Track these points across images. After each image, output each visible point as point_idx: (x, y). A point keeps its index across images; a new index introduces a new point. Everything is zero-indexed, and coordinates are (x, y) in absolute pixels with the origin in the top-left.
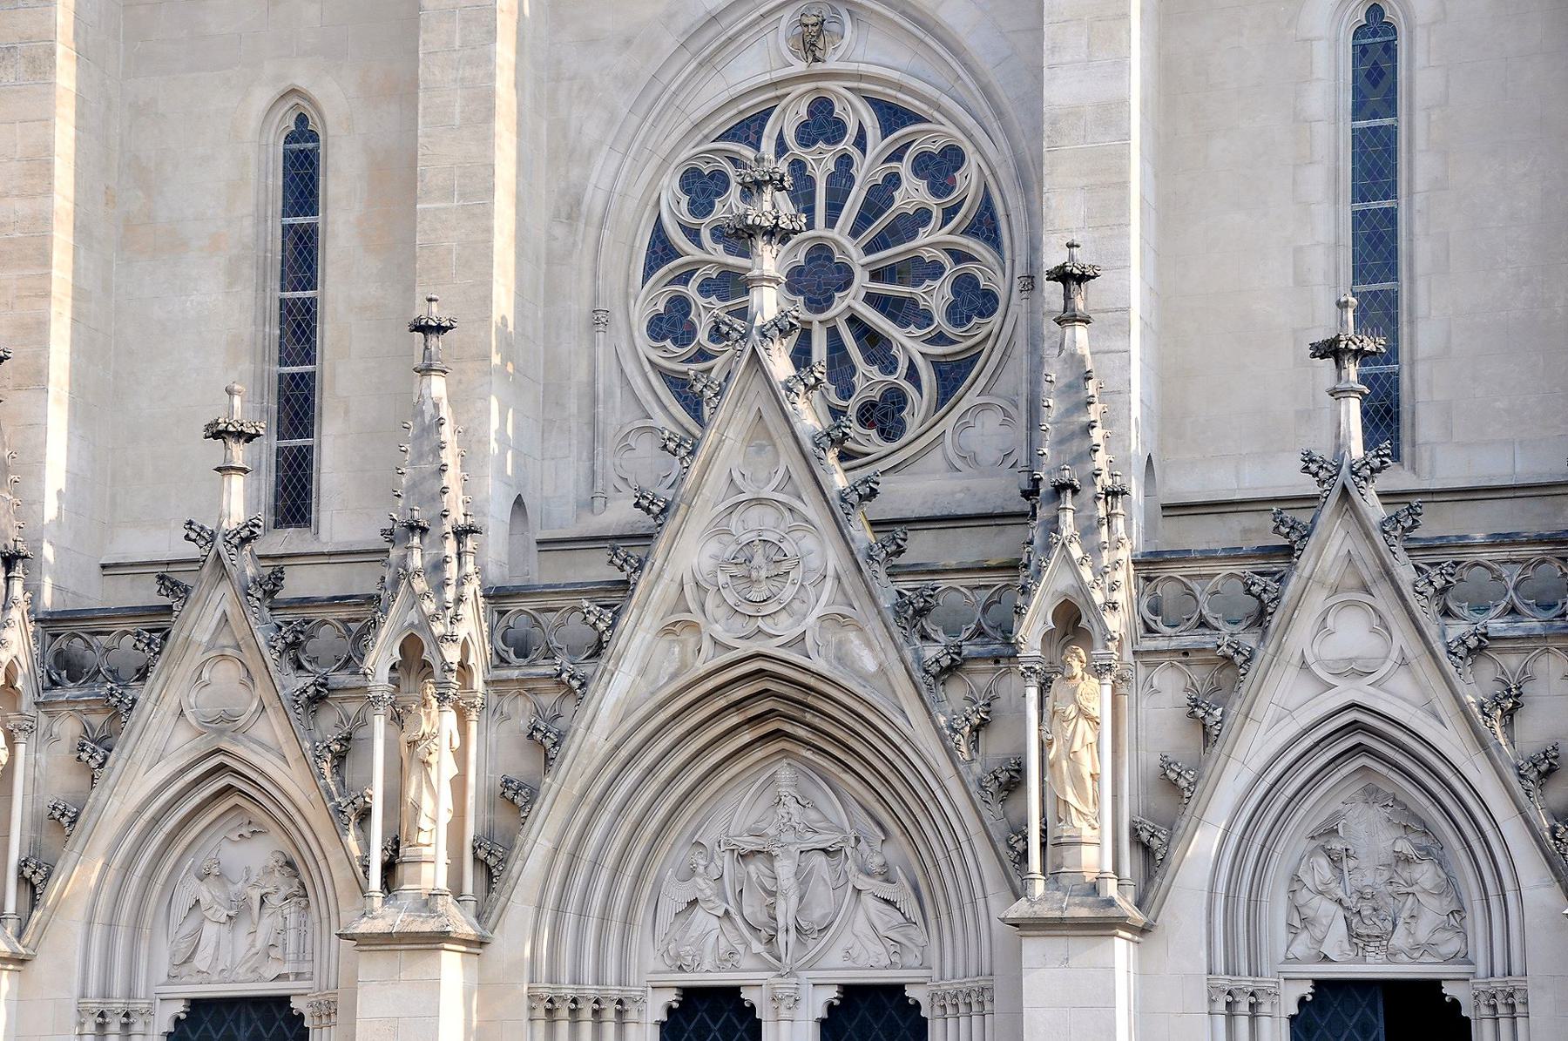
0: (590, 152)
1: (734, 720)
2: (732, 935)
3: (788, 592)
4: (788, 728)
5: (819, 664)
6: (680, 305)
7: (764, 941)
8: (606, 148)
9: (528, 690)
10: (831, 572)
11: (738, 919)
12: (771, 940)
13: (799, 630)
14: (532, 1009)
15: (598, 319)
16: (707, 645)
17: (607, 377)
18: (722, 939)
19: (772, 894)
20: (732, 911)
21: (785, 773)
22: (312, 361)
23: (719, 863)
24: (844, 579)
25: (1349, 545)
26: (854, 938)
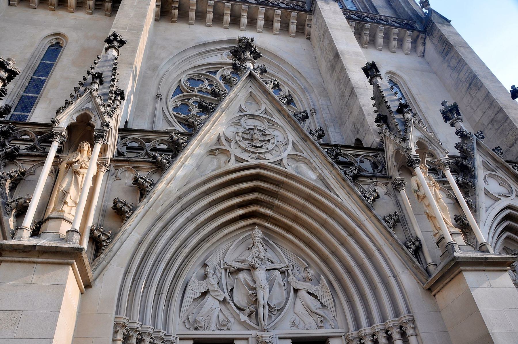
0: (163, 59)
1: (237, 200)
2: (226, 313)
3: (270, 146)
4: (263, 210)
5: (290, 170)
6: (185, 105)
7: (247, 315)
8: (168, 59)
9: (134, 167)
10: (290, 140)
11: (231, 303)
12: (254, 314)
13: (279, 158)
14: (116, 332)
15: (158, 97)
16: (233, 159)
17: (159, 113)
18: (221, 315)
19: (255, 289)
20: (228, 298)
21: (258, 233)
22: (37, 93)
23: (219, 275)
24: (297, 143)
25: (481, 159)
26: (295, 315)
